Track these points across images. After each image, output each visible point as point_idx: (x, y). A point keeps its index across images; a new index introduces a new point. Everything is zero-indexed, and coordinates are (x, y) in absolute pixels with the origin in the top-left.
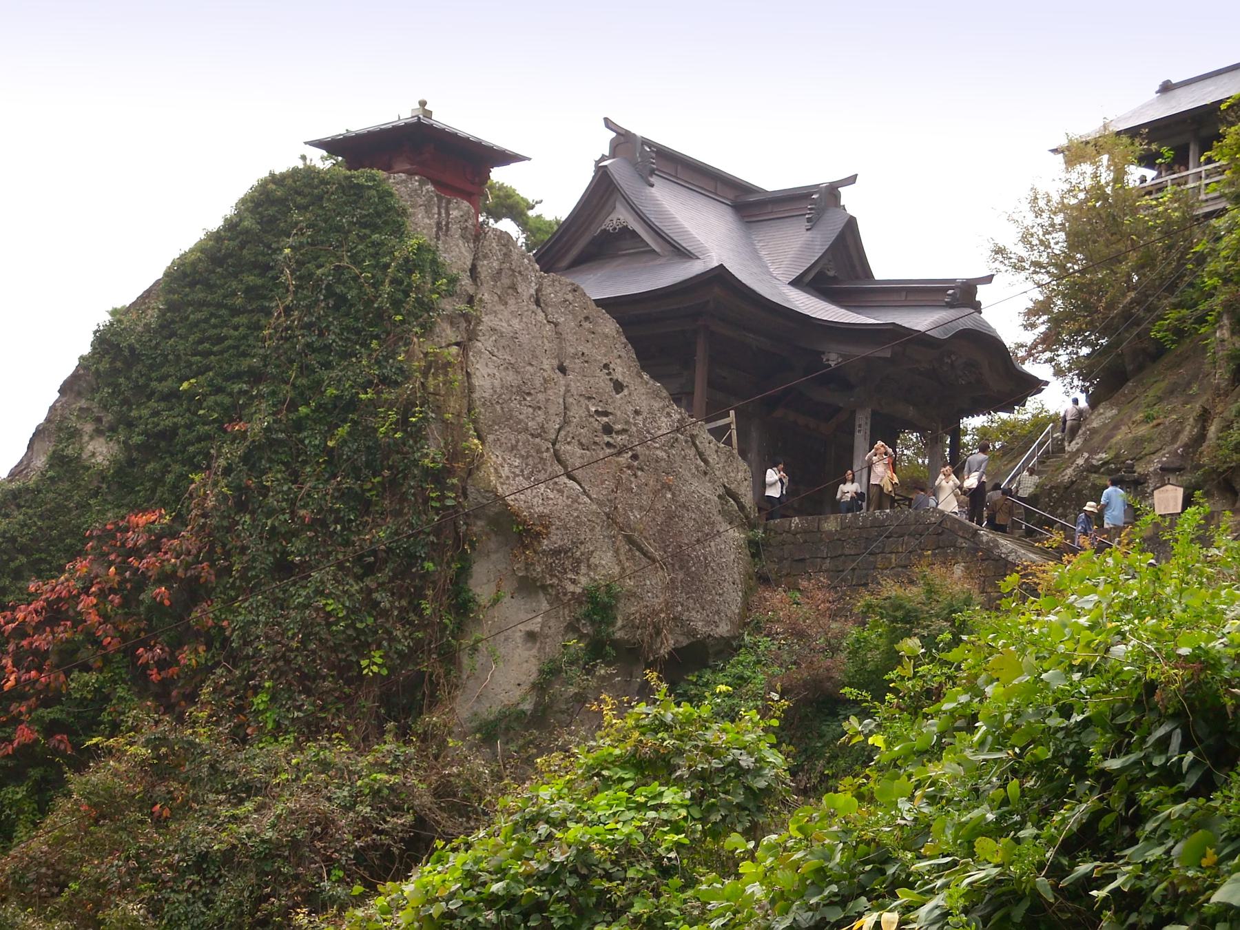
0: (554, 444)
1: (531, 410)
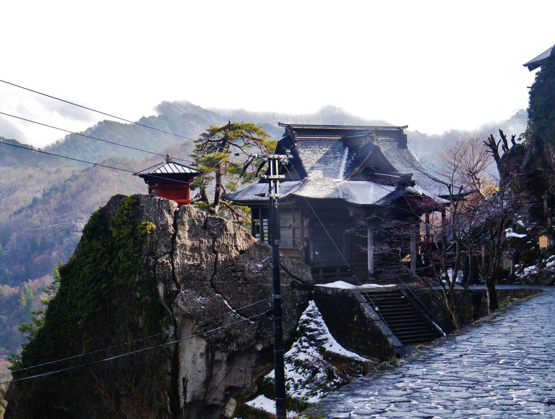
0: (211, 281)
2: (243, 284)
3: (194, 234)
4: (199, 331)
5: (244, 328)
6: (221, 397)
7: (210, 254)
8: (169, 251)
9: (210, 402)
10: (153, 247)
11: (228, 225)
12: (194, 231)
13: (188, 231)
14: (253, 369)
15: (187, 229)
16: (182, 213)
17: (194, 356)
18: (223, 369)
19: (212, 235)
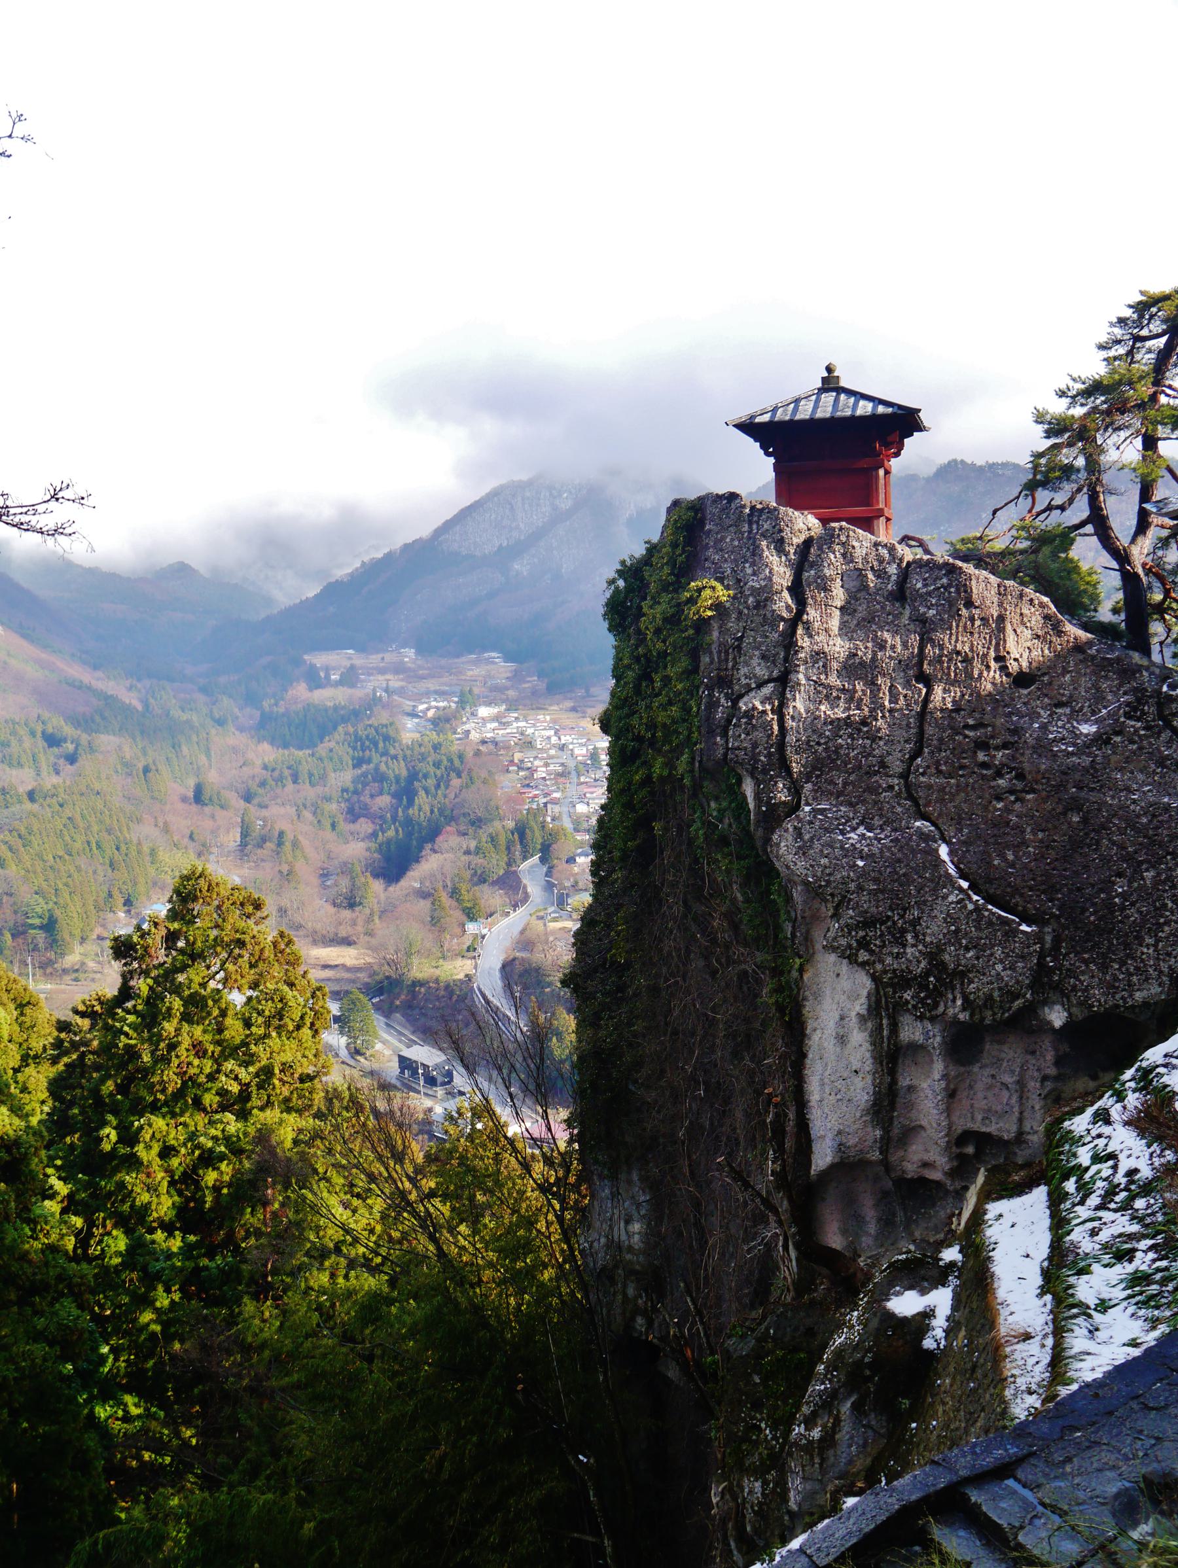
0: (905, 776)
1: (869, 742)
2: (1011, 792)
3: (857, 618)
4: (843, 942)
5: (993, 946)
6: (942, 1162)
7: (907, 684)
8: (775, 674)
9: (911, 1169)
10: (727, 660)
11: (976, 589)
12: (862, 610)
13: (842, 609)
14: (1049, 1085)
15: (839, 604)
16: (820, 548)
17: (842, 1018)
18: (937, 1076)
19: (922, 621)
